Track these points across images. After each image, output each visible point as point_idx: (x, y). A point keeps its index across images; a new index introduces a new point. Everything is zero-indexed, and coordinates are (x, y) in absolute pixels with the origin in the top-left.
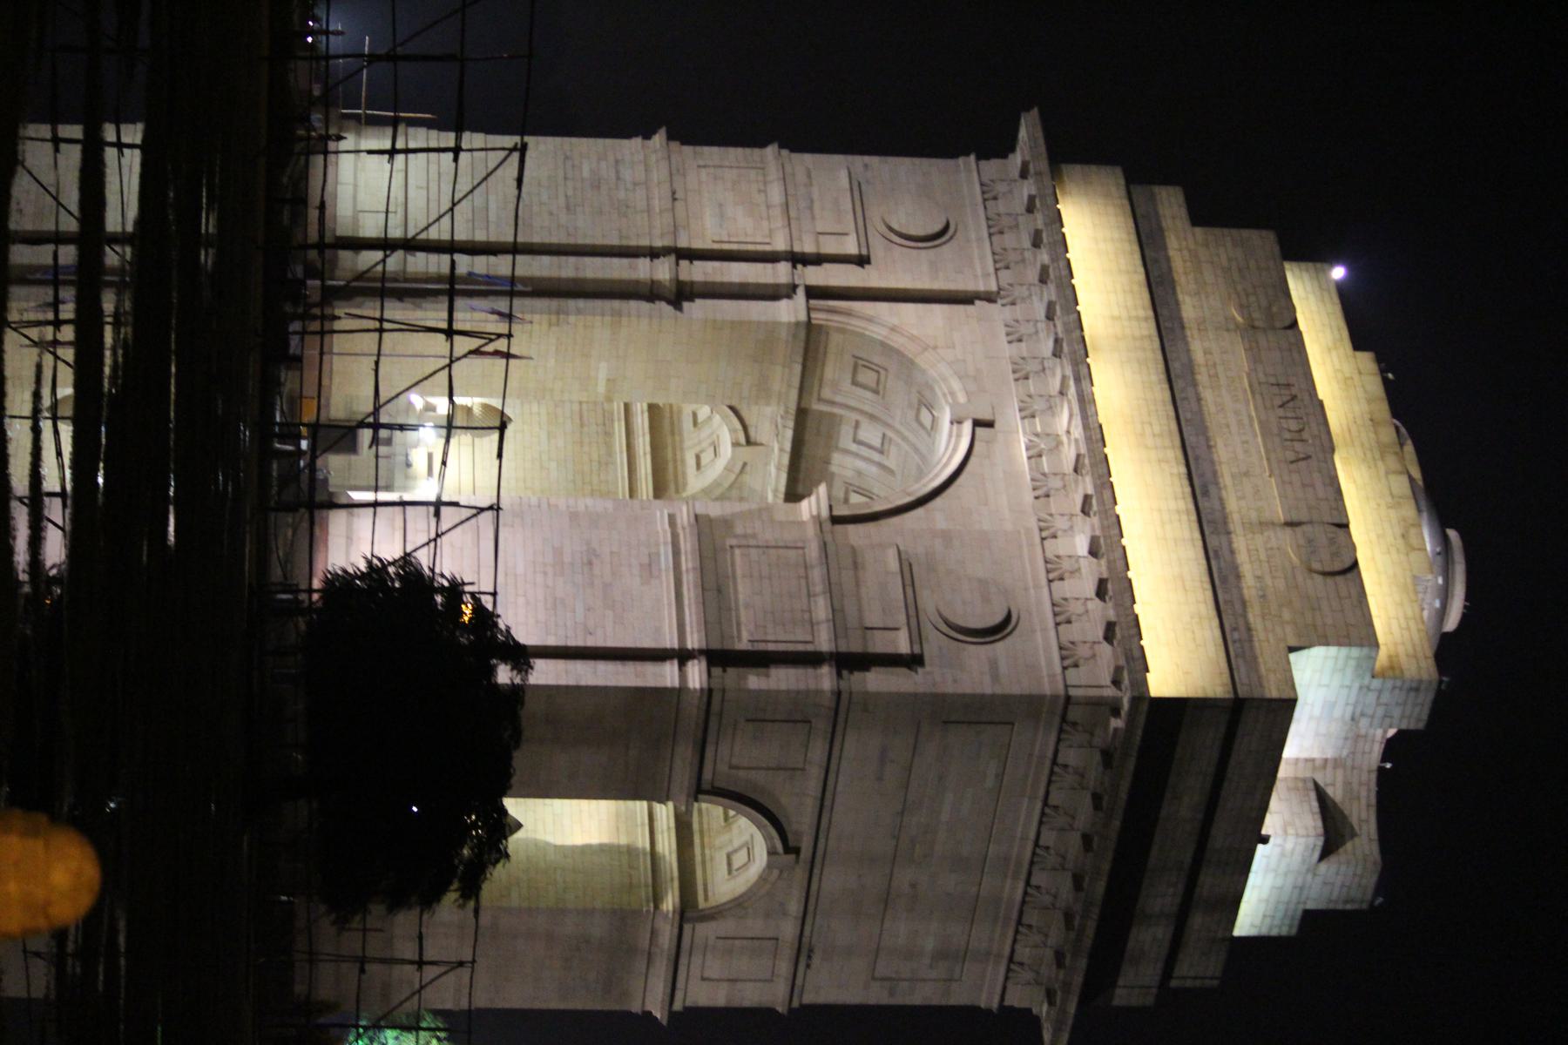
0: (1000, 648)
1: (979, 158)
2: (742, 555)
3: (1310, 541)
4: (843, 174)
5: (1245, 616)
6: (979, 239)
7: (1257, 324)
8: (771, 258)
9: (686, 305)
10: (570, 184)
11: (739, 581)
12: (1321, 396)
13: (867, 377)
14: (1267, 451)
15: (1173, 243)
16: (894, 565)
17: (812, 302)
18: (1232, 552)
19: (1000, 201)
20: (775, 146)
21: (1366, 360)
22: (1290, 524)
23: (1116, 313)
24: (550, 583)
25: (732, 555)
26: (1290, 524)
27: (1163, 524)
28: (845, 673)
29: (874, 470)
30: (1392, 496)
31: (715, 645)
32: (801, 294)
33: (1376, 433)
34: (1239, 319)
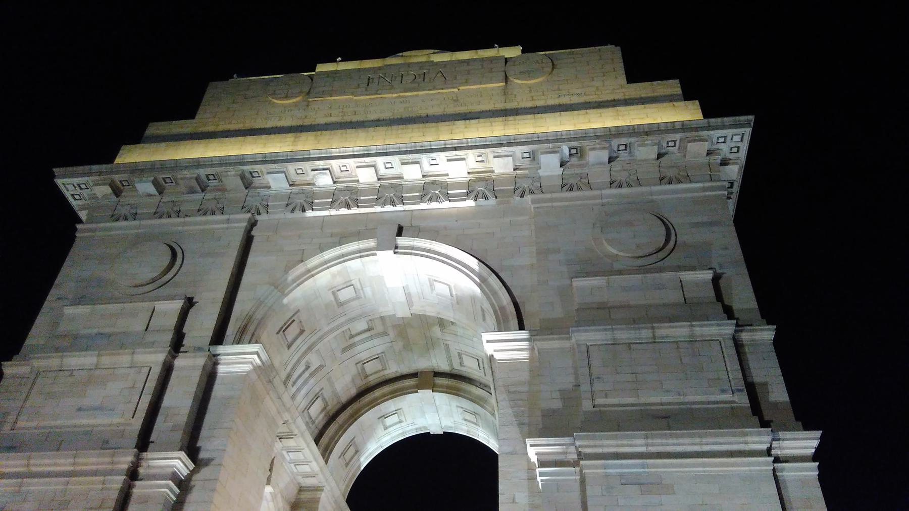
0: (675, 220)
2: (606, 396)
4: (69, 311)
6: (184, 224)
7: (306, 90)
8: (167, 370)
9: (202, 455)
11: (643, 400)
13: (293, 331)
14: (434, 88)
15: (210, 128)
22: (506, 79)
25: (600, 406)
26: (506, 79)
29: (312, 381)
32: (220, 349)
34: (298, 99)
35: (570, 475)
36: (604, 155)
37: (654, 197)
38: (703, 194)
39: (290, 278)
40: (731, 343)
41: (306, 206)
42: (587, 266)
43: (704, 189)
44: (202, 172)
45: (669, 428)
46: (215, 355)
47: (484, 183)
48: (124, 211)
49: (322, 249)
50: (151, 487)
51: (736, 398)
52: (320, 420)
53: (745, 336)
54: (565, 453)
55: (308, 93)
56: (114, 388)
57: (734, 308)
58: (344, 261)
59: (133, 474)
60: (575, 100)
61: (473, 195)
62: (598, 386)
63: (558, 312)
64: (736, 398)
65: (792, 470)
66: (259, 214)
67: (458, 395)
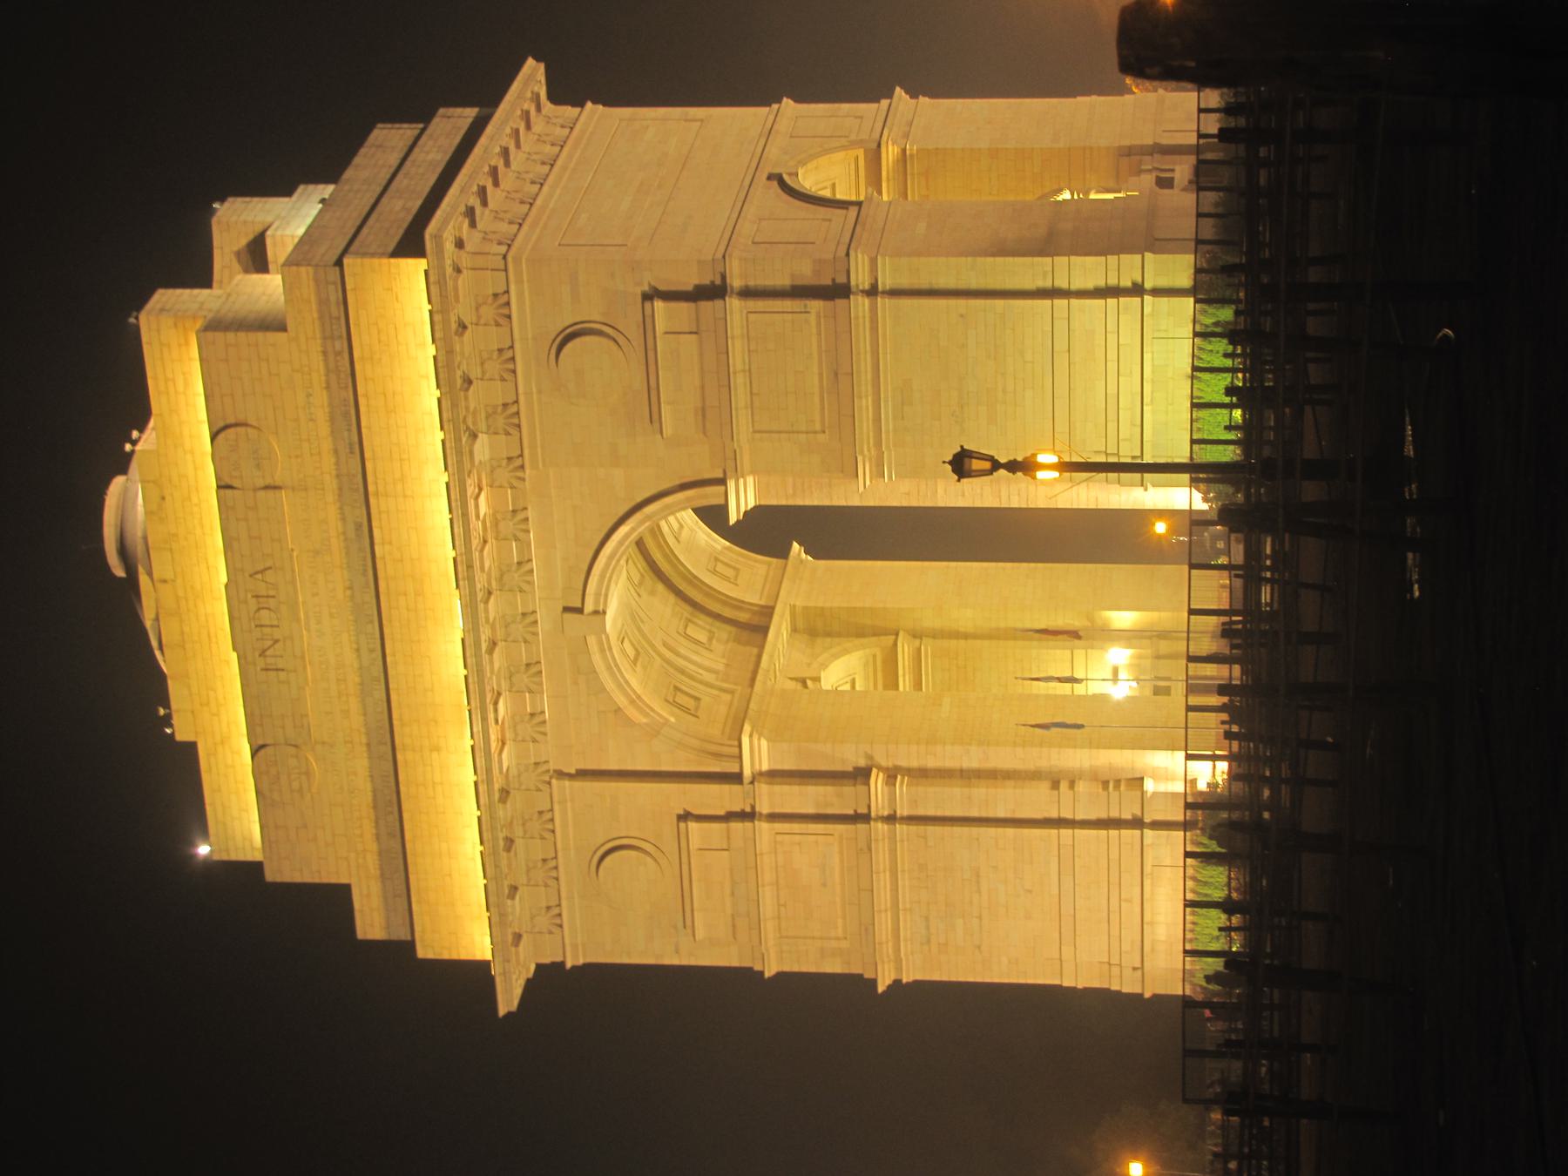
0: (567, 317)
1: (562, 964)
3: (258, 466)
5: (328, 371)
7: (292, 750)
8: (773, 817)
11: (816, 390)
12: (234, 655)
14: (293, 582)
15: (372, 862)
17: (736, 770)
18: (336, 451)
19: (544, 904)
20: (767, 975)
21: (182, 731)
23: (435, 755)
27: (403, 479)
29: (682, 651)
31: (840, 302)
32: (747, 772)
33: (182, 633)
41: (540, 719)
43: (519, 282)
47: (502, 525)
48: (543, 921)
51: (813, 311)
52: (703, 620)
57: (696, 282)
59: (891, 819)
60: (321, 398)
64: (813, 311)
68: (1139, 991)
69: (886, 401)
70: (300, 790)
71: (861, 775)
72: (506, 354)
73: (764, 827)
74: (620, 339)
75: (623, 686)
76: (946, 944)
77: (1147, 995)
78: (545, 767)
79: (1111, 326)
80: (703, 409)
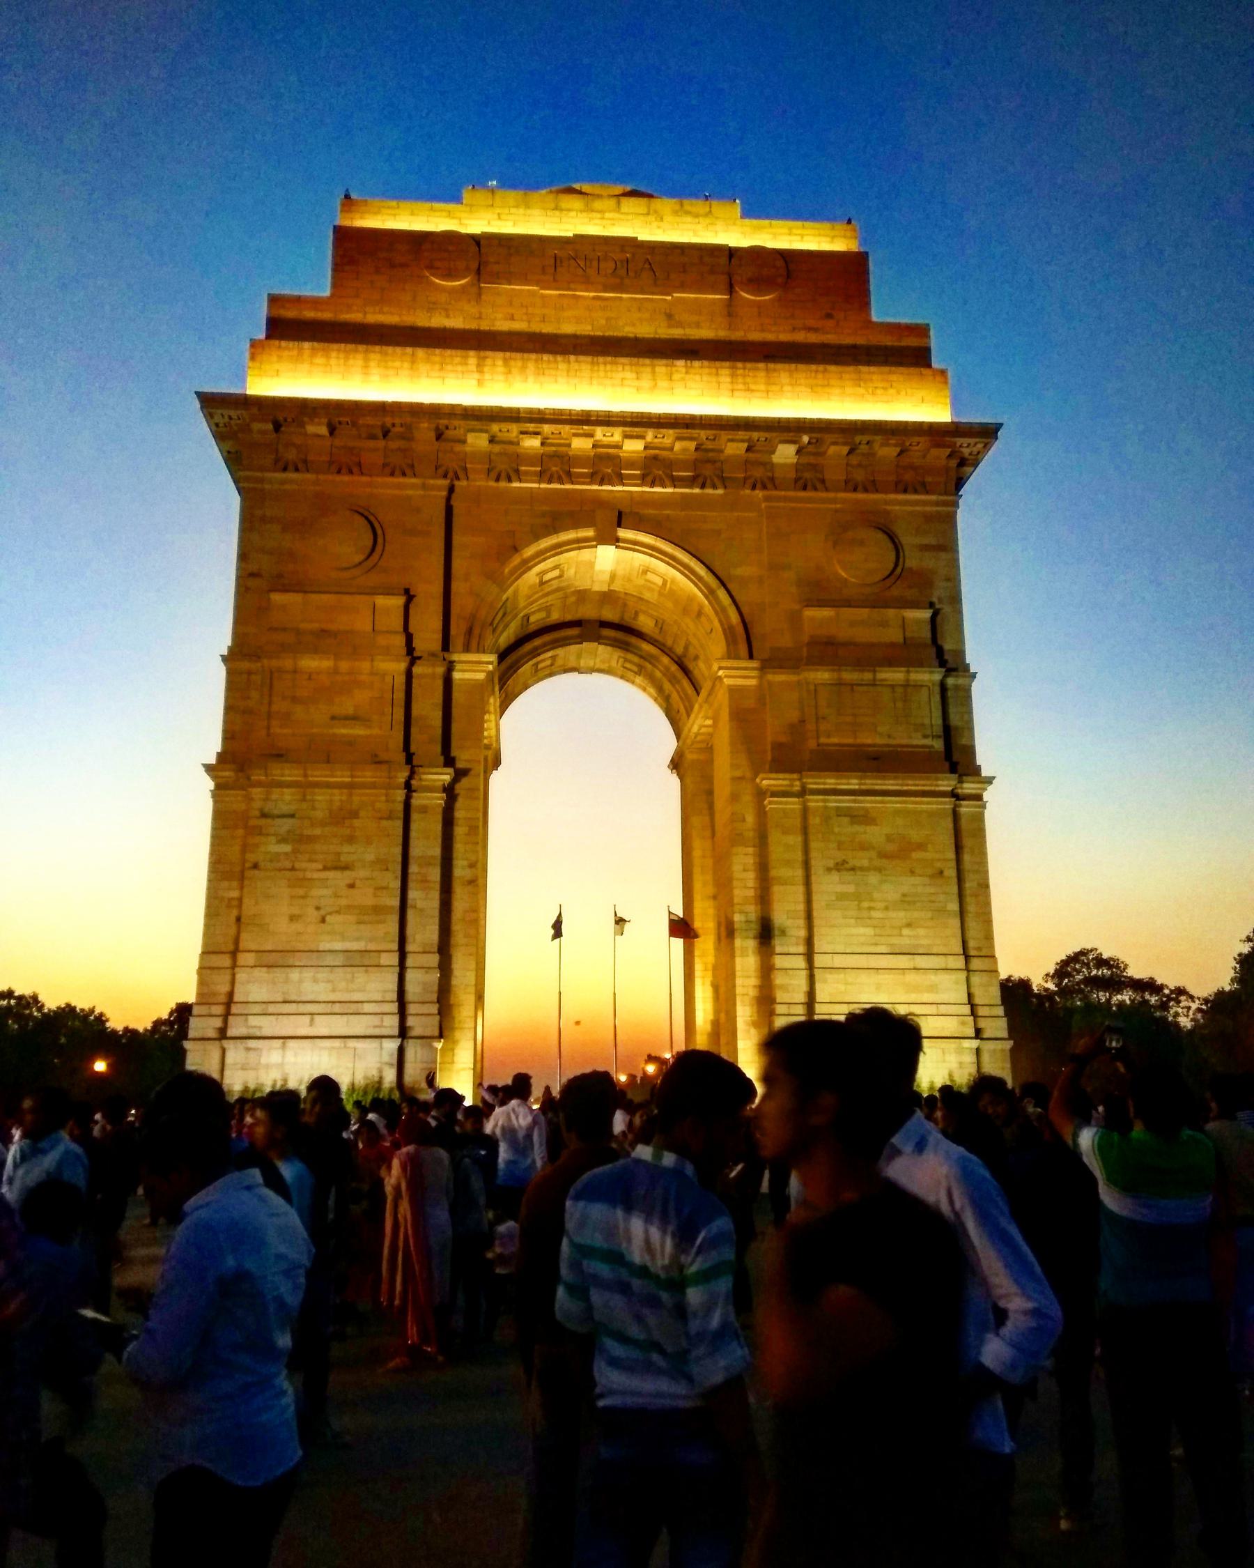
0: (907, 540)
2: (829, 737)
3: (750, 280)
4: (276, 597)
7: (474, 266)
9: (460, 765)
10: (297, 865)
11: (859, 741)
12: (571, 234)
16: (827, 613)
21: (467, 195)
22: (731, 290)
23: (475, 382)
24: (882, 905)
28: (949, 666)
30: (648, 214)
31: (947, 764)
32: (455, 657)
33: (569, 210)
35: (793, 804)
36: (845, 450)
37: (889, 508)
38: (935, 509)
39: (507, 570)
40: (937, 689)
41: (512, 474)
42: (819, 592)
43: (937, 504)
44: (388, 421)
45: (878, 771)
46: (451, 663)
47: (709, 466)
48: (291, 455)
49: (537, 537)
50: (428, 798)
53: (950, 681)
54: (791, 785)
55: (478, 272)
56: (362, 697)
58: (562, 553)
60: (813, 338)
61: (701, 480)
62: (823, 726)
63: (786, 641)
65: (967, 806)
66: (458, 478)
67: (627, 650)
68: (191, 1034)
69: (855, 801)
70: (430, 267)
71: (449, 761)
72: (871, 486)
73: (403, 666)
74: (892, 579)
75: (541, 556)
76: (260, 834)
77: (187, 1045)
78: (461, 475)
79: (943, 1009)
80: (833, 644)
